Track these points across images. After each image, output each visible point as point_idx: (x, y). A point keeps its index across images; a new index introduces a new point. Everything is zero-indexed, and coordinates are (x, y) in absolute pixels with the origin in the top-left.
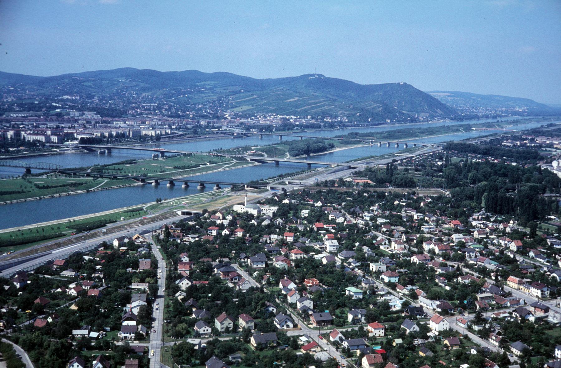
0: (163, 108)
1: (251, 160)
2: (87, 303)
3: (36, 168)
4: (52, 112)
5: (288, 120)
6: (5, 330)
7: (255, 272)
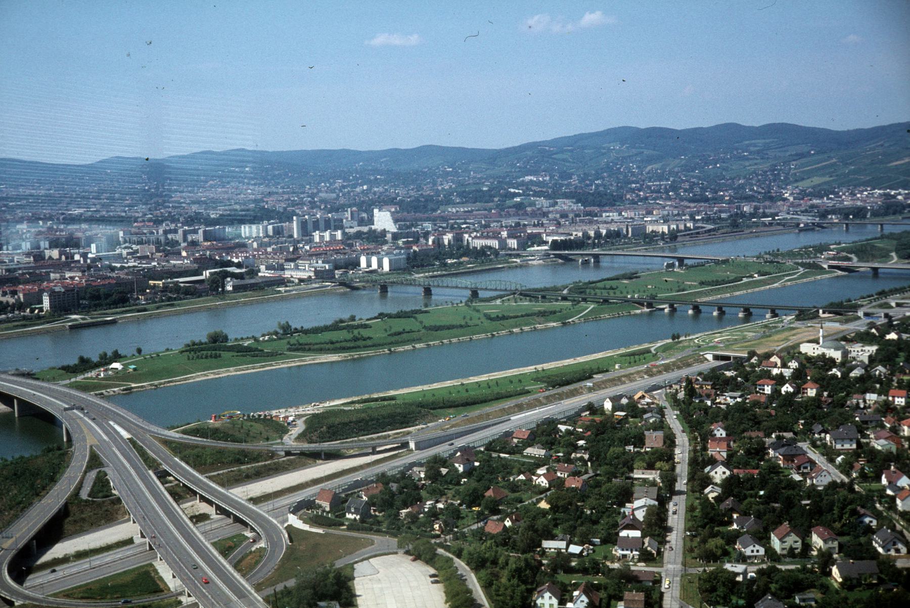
0: (681, 188)
1: (830, 267)
2: (564, 500)
3: (486, 289)
4: (509, 203)
5: (894, 197)
6: (442, 536)
7: (839, 456)
